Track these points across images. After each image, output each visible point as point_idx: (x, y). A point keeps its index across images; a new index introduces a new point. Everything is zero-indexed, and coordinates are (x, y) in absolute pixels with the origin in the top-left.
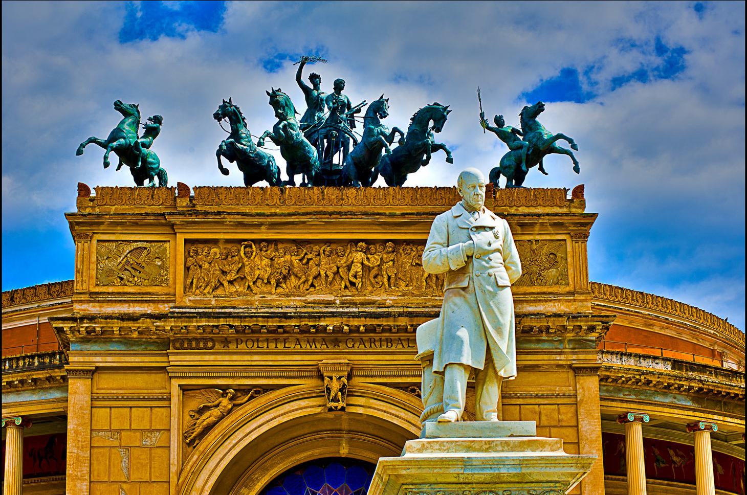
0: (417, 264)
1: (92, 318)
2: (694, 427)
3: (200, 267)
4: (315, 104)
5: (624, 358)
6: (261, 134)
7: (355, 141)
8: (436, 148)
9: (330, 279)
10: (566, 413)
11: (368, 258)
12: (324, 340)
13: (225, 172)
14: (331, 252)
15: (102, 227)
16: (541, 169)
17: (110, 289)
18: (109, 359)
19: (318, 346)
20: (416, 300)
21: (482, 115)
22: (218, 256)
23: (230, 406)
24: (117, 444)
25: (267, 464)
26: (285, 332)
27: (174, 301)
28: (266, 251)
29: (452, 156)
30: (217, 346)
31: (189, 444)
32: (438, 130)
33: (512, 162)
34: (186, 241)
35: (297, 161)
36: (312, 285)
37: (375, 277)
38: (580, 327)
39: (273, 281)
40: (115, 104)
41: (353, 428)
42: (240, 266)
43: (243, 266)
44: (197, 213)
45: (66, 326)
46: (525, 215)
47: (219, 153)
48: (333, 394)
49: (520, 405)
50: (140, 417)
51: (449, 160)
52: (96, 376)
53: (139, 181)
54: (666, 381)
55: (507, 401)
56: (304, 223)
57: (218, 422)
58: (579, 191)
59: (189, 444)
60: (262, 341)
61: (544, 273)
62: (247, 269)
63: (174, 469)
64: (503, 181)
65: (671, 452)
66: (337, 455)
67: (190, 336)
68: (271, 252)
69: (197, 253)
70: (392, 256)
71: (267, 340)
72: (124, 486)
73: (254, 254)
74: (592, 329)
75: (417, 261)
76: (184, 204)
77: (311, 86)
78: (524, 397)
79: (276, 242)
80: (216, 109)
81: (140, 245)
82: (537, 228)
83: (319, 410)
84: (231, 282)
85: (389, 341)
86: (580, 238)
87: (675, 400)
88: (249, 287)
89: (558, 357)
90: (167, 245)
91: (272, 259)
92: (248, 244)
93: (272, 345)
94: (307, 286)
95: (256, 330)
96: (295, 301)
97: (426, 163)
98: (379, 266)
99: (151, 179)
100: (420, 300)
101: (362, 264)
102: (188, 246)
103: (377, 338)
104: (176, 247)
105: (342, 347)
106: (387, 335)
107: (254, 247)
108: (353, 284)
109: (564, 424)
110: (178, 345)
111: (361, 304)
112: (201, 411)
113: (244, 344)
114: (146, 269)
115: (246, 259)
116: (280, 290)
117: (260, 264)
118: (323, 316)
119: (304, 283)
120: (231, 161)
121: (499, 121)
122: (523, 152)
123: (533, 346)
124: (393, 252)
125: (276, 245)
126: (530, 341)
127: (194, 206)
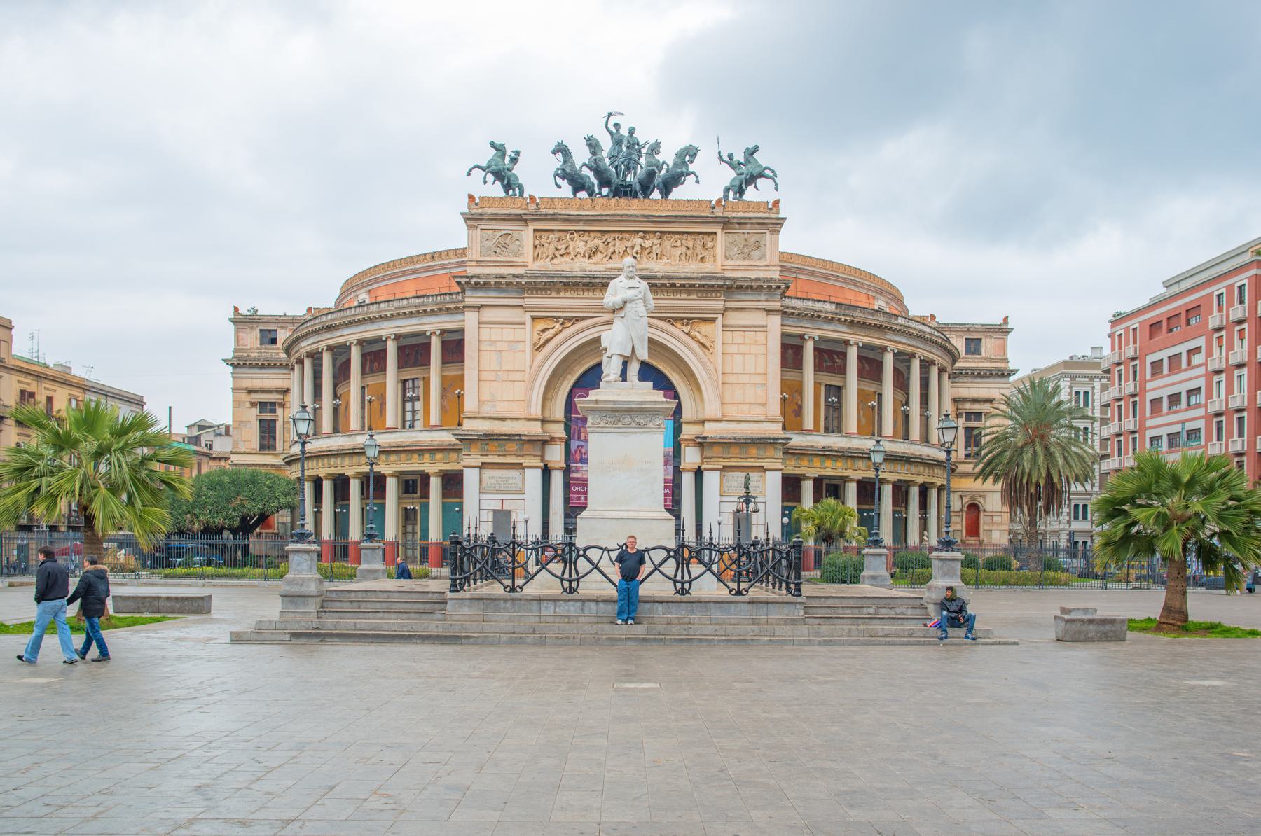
1: (478, 277)
2: (847, 343)
4: (618, 142)
6: (581, 164)
7: (642, 168)
8: (688, 174)
13: (559, 187)
15: (483, 221)
16: (756, 187)
17: (489, 259)
20: (672, 268)
21: (719, 153)
25: (583, 362)
26: (593, 286)
27: (527, 266)
29: (700, 179)
31: (537, 350)
32: (692, 162)
33: (737, 183)
34: (535, 230)
35: (605, 181)
36: (610, 258)
37: (649, 253)
38: (771, 286)
39: (587, 255)
45: (463, 281)
46: (741, 218)
47: (556, 175)
50: (508, 334)
51: (697, 182)
52: (481, 309)
53: (507, 192)
54: (830, 316)
55: (725, 329)
56: (606, 220)
58: (776, 203)
59: (537, 350)
61: (752, 253)
62: (571, 248)
63: (528, 364)
64: (731, 194)
65: (835, 357)
68: (586, 238)
69: (541, 237)
70: (659, 241)
71: (583, 290)
72: (499, 373)
74: (779, 287)
77: (615, 131)
78: (736, 326)
79: (589, 231)
81: (506, 232)
82: (749, 226)
84: (561, 255)
89: (757, 304)
90: (523, 232)
92: (572, 232)
93: (586, 294)
94: (607, 258)
95: (576, 285)
96: (600, 267)
97: (683, 183)
99: (514, 190)
100: (676, 268)
102: (538, 234)
104: (527, 235)
112: (543, 331)
116: (591, 261)
117: (579, 245)
119: (606, 256)
121: (731, 156)
122: (743, 177)
123: (743, 297)
126: (740, 294)
127: (539, 209)
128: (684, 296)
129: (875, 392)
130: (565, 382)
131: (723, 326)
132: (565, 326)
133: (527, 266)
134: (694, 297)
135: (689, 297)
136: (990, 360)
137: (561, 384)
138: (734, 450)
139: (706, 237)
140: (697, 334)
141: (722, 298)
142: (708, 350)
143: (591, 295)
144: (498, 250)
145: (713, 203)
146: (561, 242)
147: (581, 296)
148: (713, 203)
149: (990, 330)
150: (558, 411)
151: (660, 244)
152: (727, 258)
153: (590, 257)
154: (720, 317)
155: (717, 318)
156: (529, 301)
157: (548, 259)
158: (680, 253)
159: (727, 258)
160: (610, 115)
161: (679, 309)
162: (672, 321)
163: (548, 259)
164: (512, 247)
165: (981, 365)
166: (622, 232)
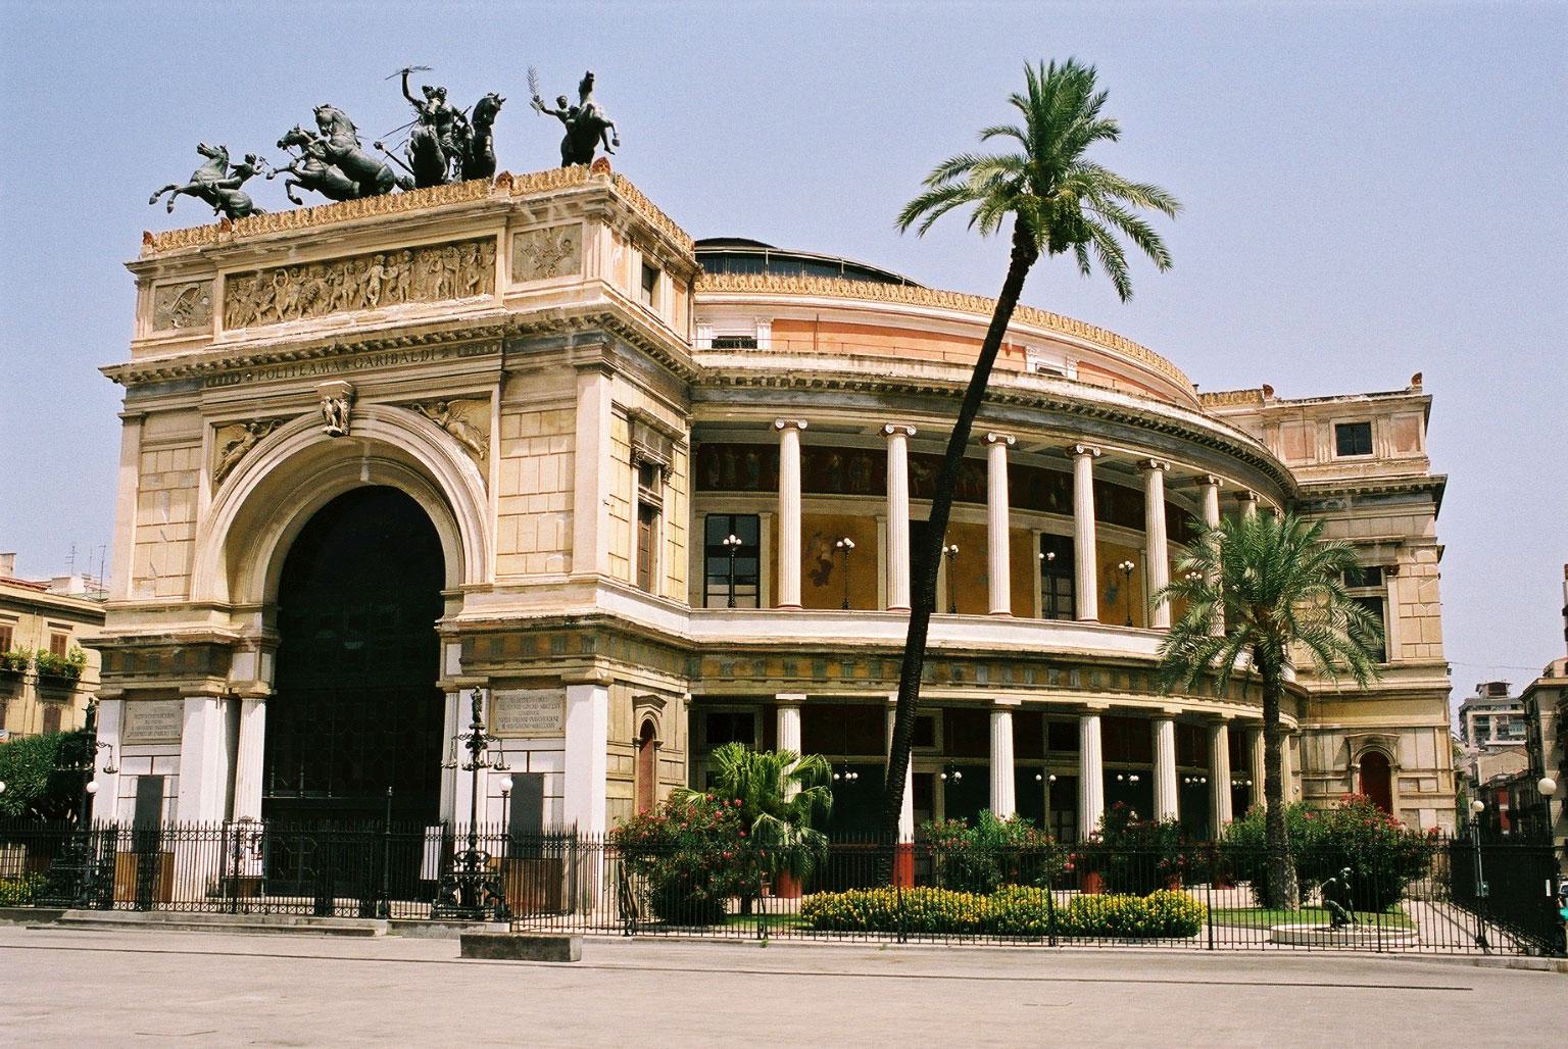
0: (433, 271)
3: (239, 301)
9: (351, 298)
10: (567, 420)
11: (385, 272)
13: (298, 202)
14: (355, 270)
18: (155, 403)
19: (330, 369)
21: (536, 99)
23: (253, 441)
24: (159, 486)
30: (242, 380)
34: (228, 277)
37: (394, 289)
40: (199, 148)
41: (374, 453)
43: (275, 295)
44: (237, 246)
48: (328, 419)
49: (521, 414)
50: (181, 458)
52: (148, 421)
55: (506, 411)
57: (242, 457)
60: (282, 370)
62: (277, 298)
66: (358, 485)
67: (219, 372)
68: (301, 279)
71: (286, 369)
73: (286, 282)
75: (433, 268)
76: (225, 239)
79: (307, 265)
80: (282, 136)
84: (264, 314)
85: (395, 357)
86: (595, 218)
87: (850, 401)
88: (279, 317)
90: (214, 283)
98: (397, 277)
102: (232, 282)
106: (390, 350)
107: (286, 273)
108: (369, 299)
109: (564, 431)
110: (210, 383)
112: (231, 446)
115: (277, 288)
117: (290, 293)
119: (329, 305)
120: (311, 190)
121: (561, 102)
124: (412, 260)
125: (307, 269)
128: (438, 358)
129: (1030, 532)
130: (270, 536)
131: (502, 407)
133: (212, 339)
134: (453, 357)
137: (262, 540)
139: (483, 246)
140: (460, 428)
142: (478, 453)
143: (297, 373)
146: (265, 290)
149: (1386, 402)
150: (256, 586)
152: (516, 279)
153: (304, 311)
154: (496, 389)
155: (491, 392)
156: (208, 397)
157: (245, 323)
158: (439, 282)
159: (516, 279)
160: (406, 73)
161: (430, 384)
162: (418, 406)
164: (198, 309)
166: (354, 258)
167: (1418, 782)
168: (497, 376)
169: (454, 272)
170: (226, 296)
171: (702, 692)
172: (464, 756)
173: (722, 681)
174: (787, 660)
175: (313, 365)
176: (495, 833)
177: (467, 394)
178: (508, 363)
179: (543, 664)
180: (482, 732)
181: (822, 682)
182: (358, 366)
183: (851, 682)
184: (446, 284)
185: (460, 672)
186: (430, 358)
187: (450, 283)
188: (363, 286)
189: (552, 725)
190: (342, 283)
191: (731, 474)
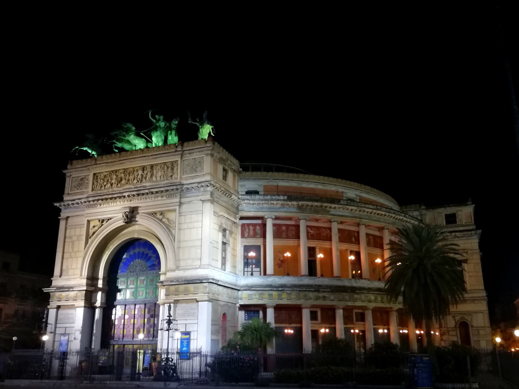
5: (265, 196)
9: (132, 180)
11: (143, 172)
12: (127, 200)
22: (103, 178)
23: (100, 225)
28: (116, 173)
30: (98, 206)
34: (94, 174)
36: (127, 183)
39: (116, 183)
42: (108, 180)
49: (185, 215)
55: (180, 214)
56: (125, 163)
62: (109, 181)
79: (119, 170)
82: (195, 153)
83: (124, 224)
89: (197, 197)
90: (90, 176)
91: (117, 176)
95: (107, 199)
101: (142, 174)
103: (142, 198)
104: (91, 178)
105: (132, 202)
110: (88, 207)
111: (140, 187)
113: (105, 204)
114: (84, 184)
115: (109, 178)
116: (118, 186)
118: (123, 192)
125: (119, 171)
126: (189, 193)
129: (347, 250)
132: (103, 224)
134: (165, 198)
135: (162, 198)
136: (463, 226)
138: (182, 287)
141: (179, 197)
143: (115, 204)
144: (78, 187)
145: (177, 145)
147: (111, 205)
148: (177, 145)
151: (151, 171)
153: (117, 185)
154: (177, 208)
155: (176, 209)
162: (153, 214)
163: (99, 189)
165: (457, 229)
167: (479, 331)
168: (178, 204)
169: (164, 172)
170: (93, 180)
171: (242, 303)
172: (166, 326)
173: (249, 299)
174: (271, 292)
175: (120, 201)
176: (174, 352)
177: (169, 210)
178: (182, 199)
179: (191, 295)
180: (171, 318)
181: (281, 299)
182: (134, 201)
183: (291, 300)
184: (162, 176)
185: (165, 298)
186: (157, 199)
187: (164, 176)
188: (136, 176)
189: (194, 315)
190: (129, 176)
191: (252, 233)
